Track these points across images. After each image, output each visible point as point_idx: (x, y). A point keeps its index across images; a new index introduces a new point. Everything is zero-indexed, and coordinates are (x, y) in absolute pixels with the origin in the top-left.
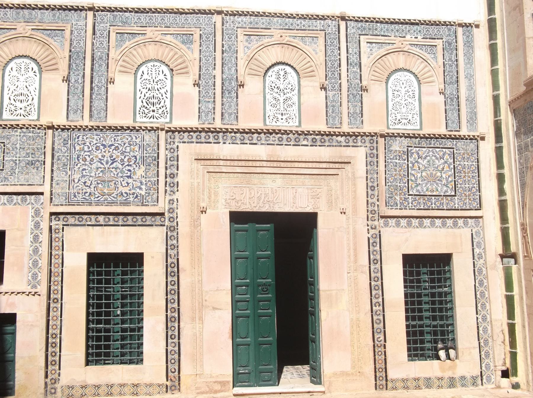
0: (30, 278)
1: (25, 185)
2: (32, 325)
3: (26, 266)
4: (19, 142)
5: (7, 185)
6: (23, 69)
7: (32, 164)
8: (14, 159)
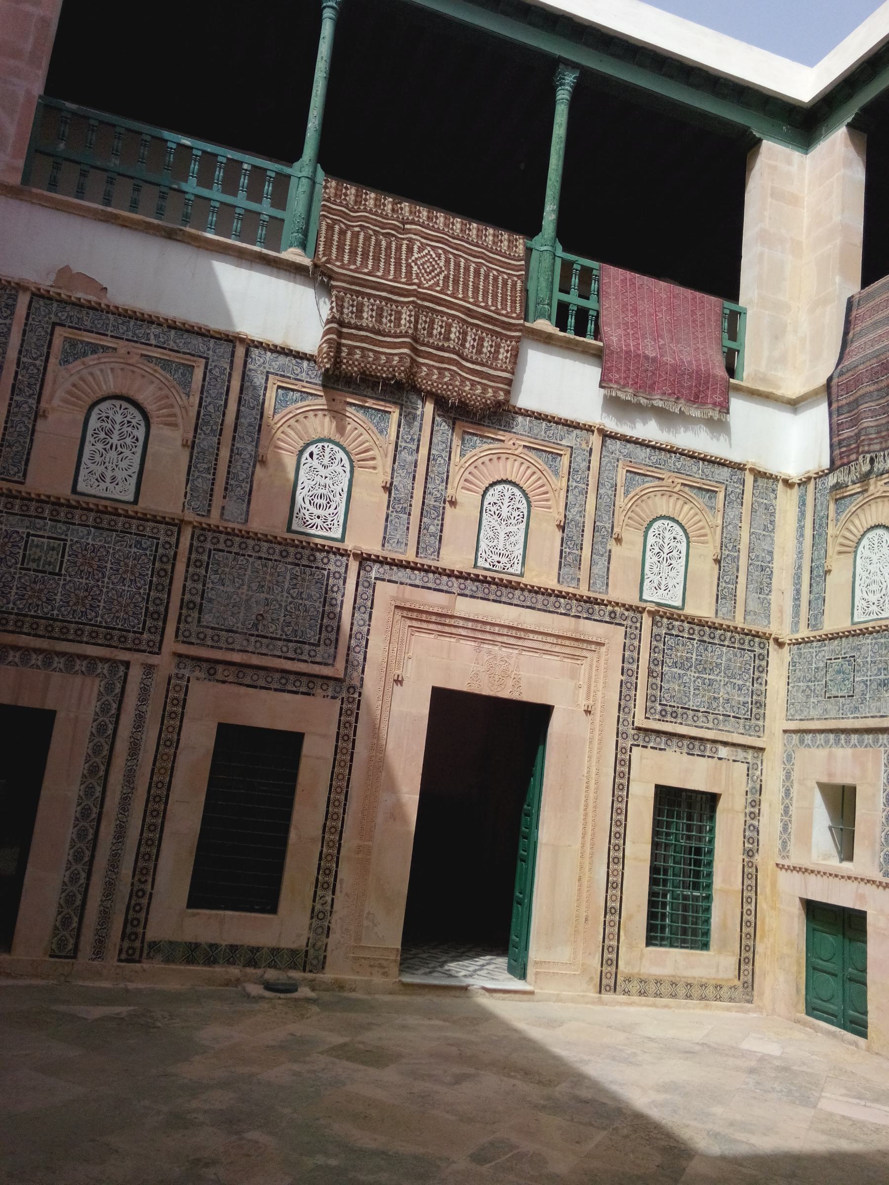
0: (882, 860)
1: (876, 717)
2: (884, 934)
3: (878, 840)
4: (870, 653)
5: (858, 718)
6: (875, 546)
7: (885, 685)
8: (865, 678)
